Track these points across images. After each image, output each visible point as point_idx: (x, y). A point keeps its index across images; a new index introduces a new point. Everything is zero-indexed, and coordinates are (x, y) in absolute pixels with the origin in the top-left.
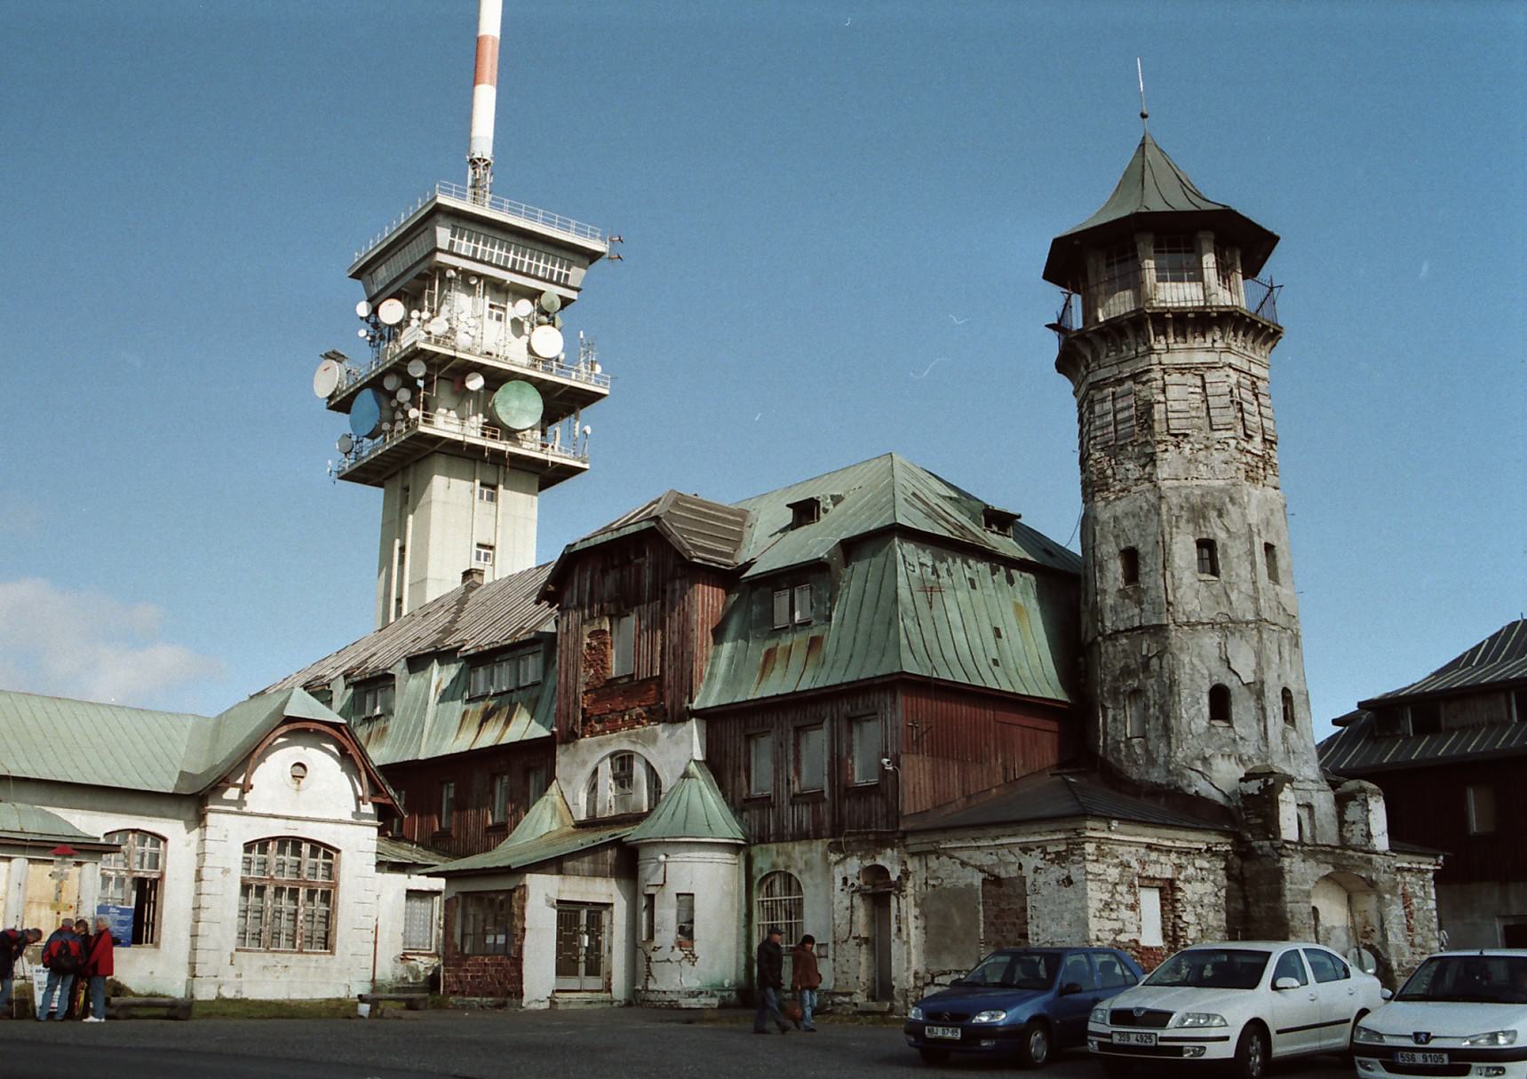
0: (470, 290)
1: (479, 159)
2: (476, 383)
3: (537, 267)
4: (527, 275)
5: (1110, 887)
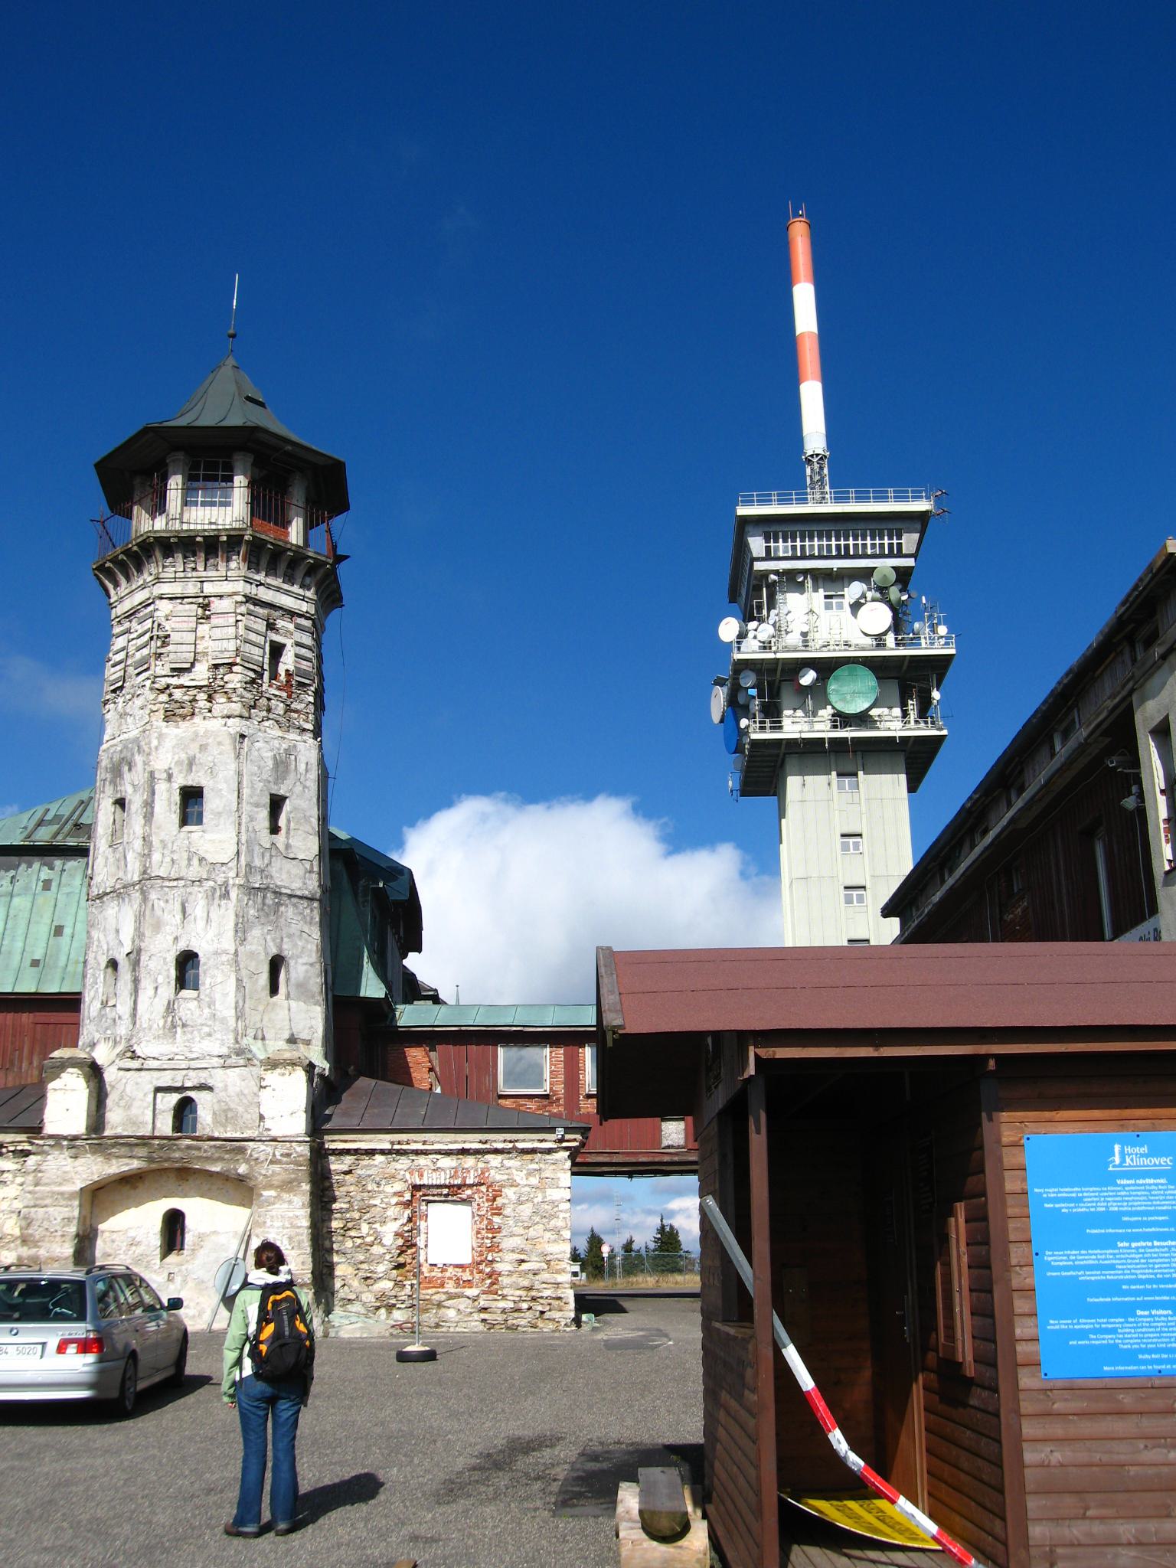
0: (800, 588)
1: (812, 456)
3: (864, 546)
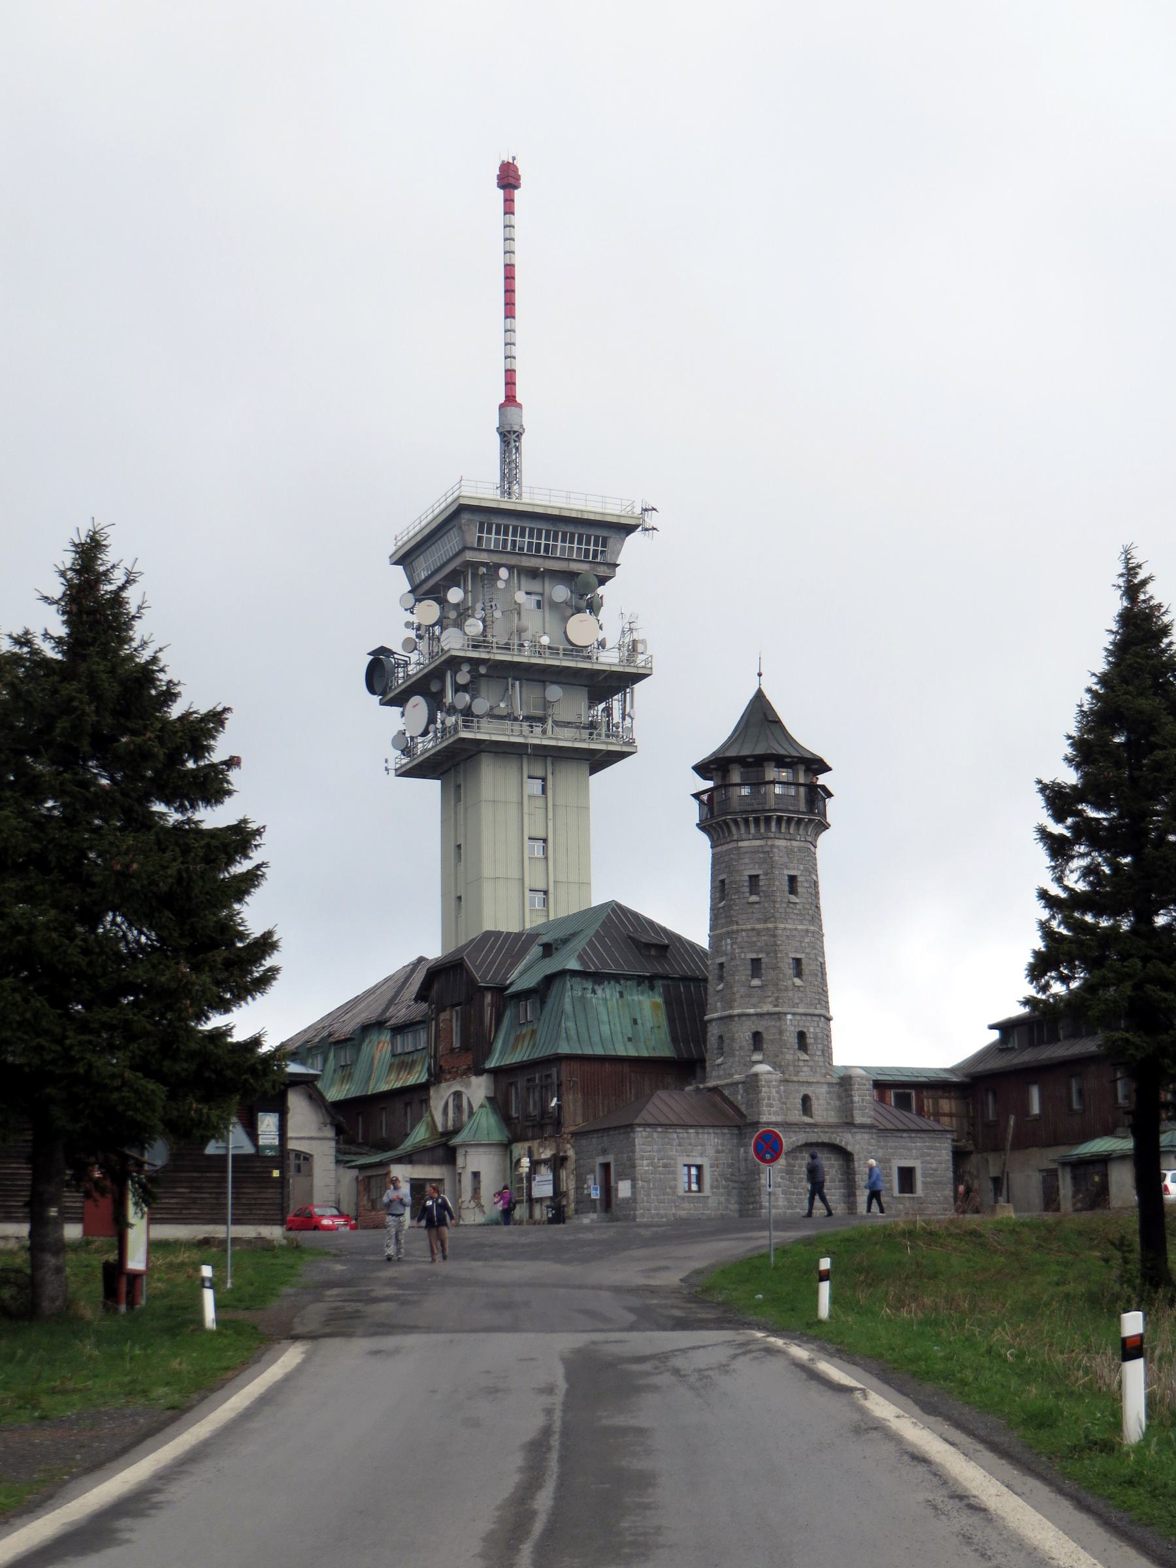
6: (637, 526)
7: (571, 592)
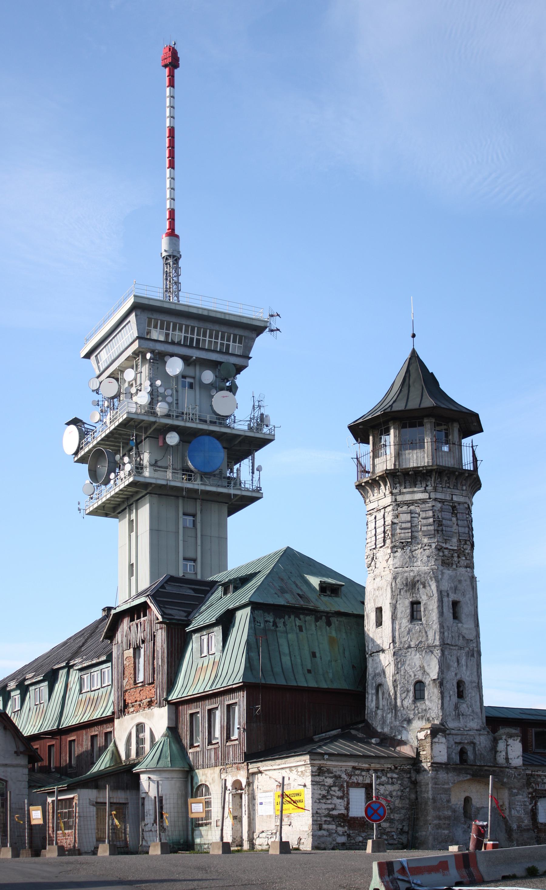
2: (173, 439)
3: (216, 343)
4: (209, 350)
5: (327, 788)
6: (266, 328)
7: (216, 376)
